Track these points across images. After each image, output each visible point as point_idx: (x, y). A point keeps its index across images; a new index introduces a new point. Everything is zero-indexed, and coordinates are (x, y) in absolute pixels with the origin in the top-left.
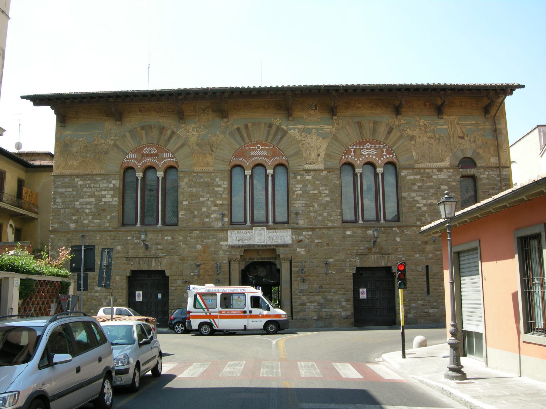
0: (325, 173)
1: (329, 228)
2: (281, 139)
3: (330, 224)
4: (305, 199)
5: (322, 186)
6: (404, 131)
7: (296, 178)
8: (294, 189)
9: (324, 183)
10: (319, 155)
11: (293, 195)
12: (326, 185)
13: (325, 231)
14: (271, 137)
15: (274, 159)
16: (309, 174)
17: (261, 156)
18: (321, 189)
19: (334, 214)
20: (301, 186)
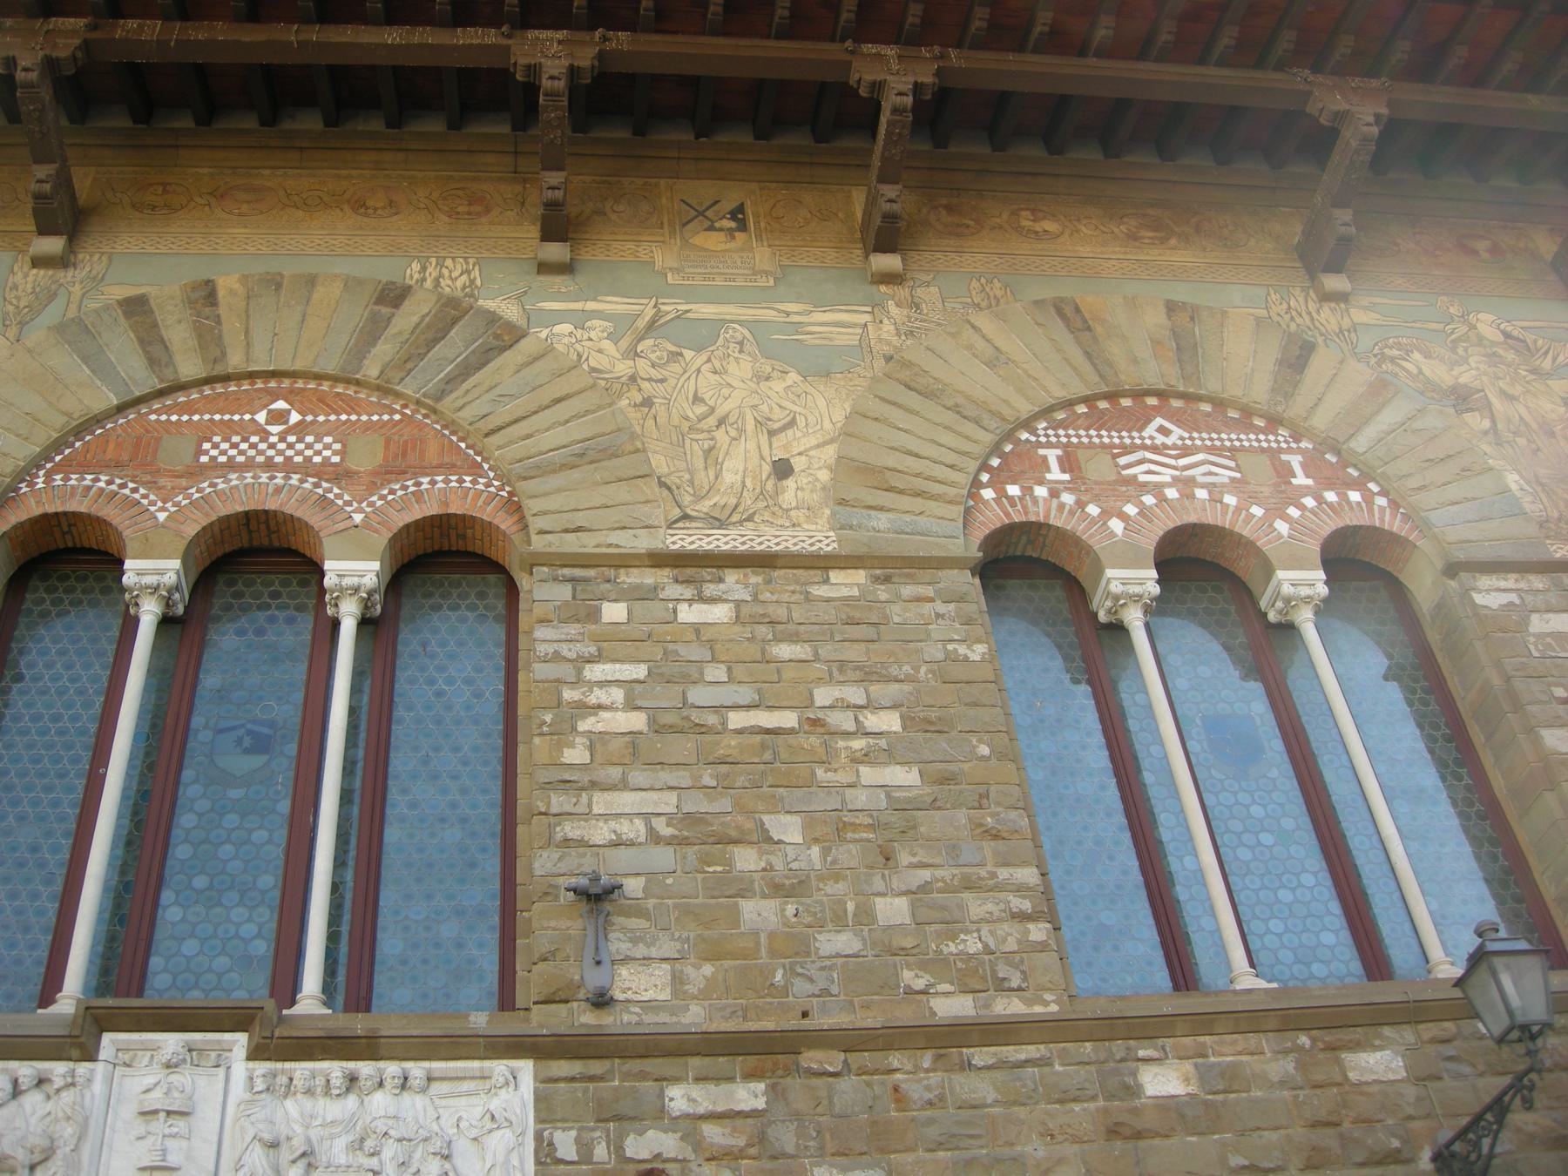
0: (846, 583)
1: (949, 1039)
2: (467, 370)
3: (952, 1006)
4: (682, 777)
5: (830, 680)
6: (1392, 360)
7: (594, 615)
8: (568, 695)
9: (854, 653)
10: (783, 469)
11: (559, 747)
12: (868, 675)
13: (916, 1075)
14: (384, 350)
15: (398, 490)
16: (710, 589)
17: (289, 467)
18: (823, 696)
19: (977, 906)
20: (641, 671)
